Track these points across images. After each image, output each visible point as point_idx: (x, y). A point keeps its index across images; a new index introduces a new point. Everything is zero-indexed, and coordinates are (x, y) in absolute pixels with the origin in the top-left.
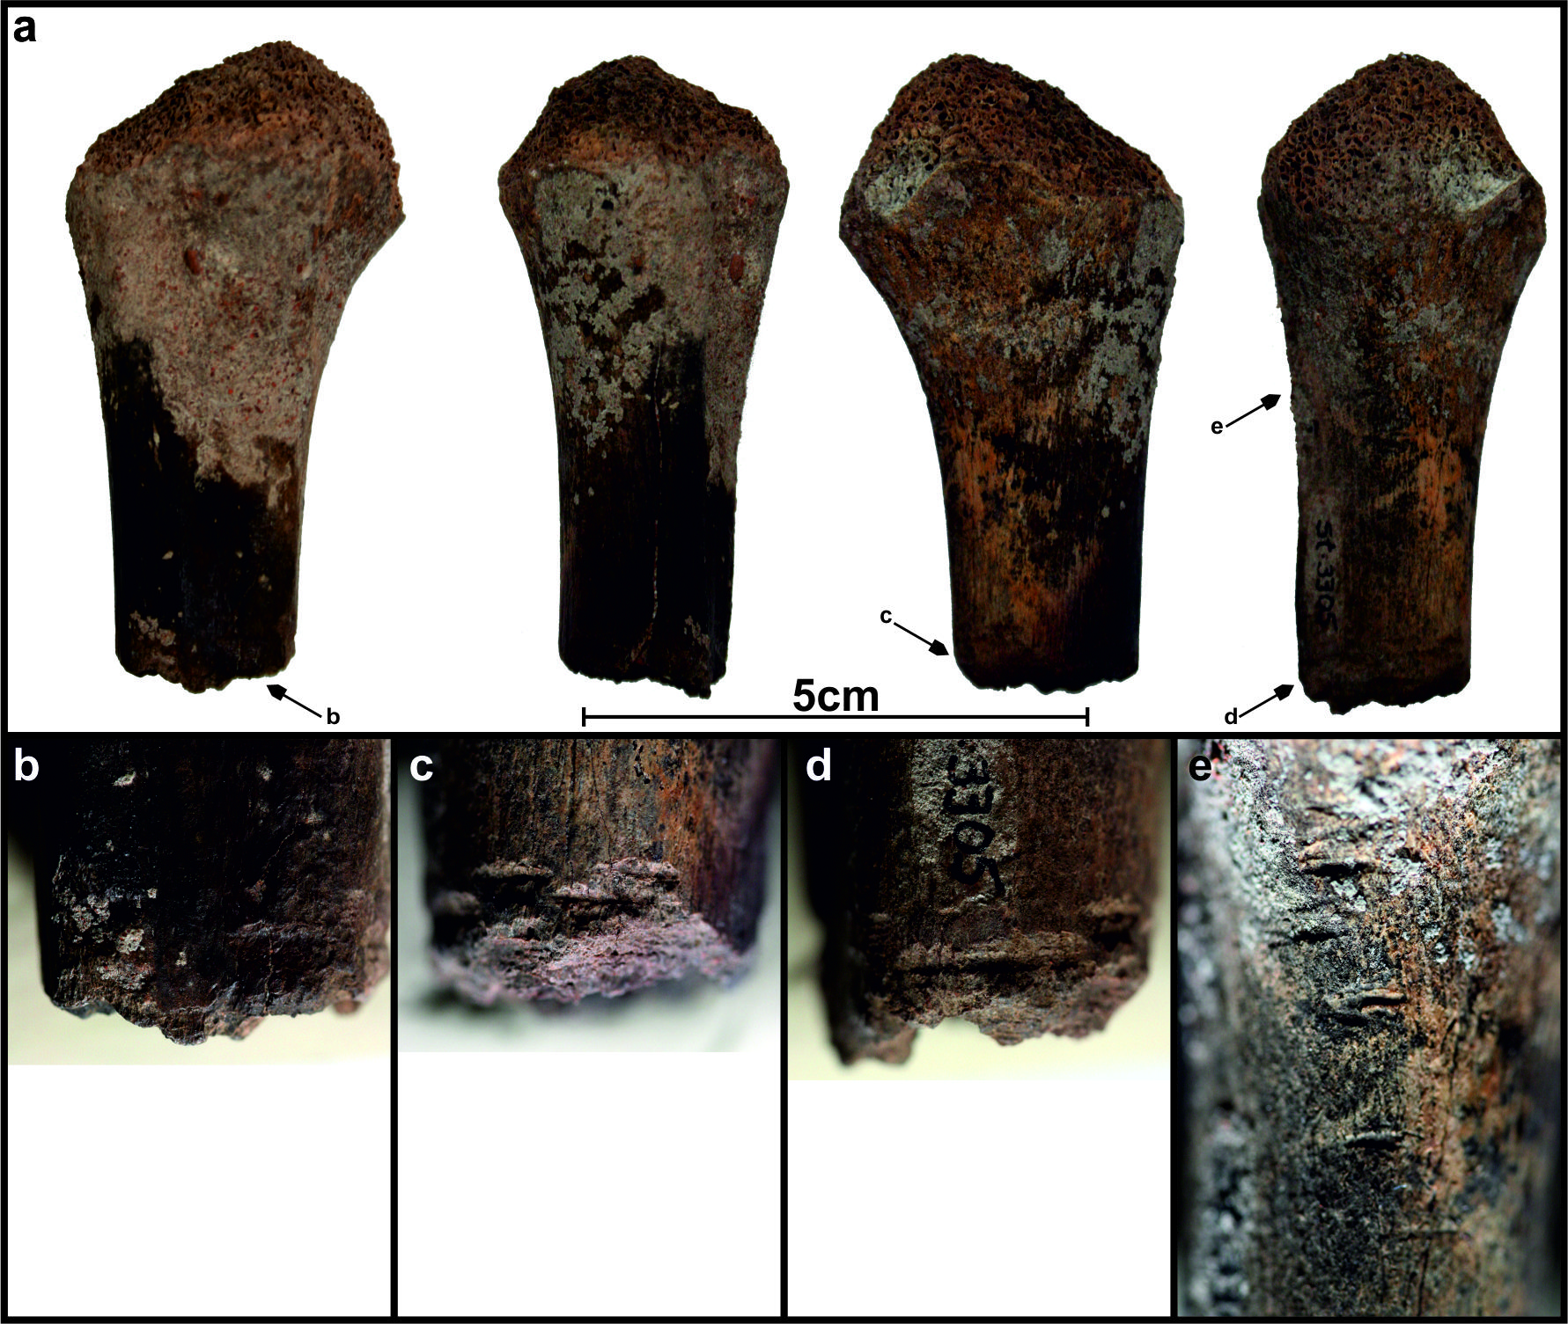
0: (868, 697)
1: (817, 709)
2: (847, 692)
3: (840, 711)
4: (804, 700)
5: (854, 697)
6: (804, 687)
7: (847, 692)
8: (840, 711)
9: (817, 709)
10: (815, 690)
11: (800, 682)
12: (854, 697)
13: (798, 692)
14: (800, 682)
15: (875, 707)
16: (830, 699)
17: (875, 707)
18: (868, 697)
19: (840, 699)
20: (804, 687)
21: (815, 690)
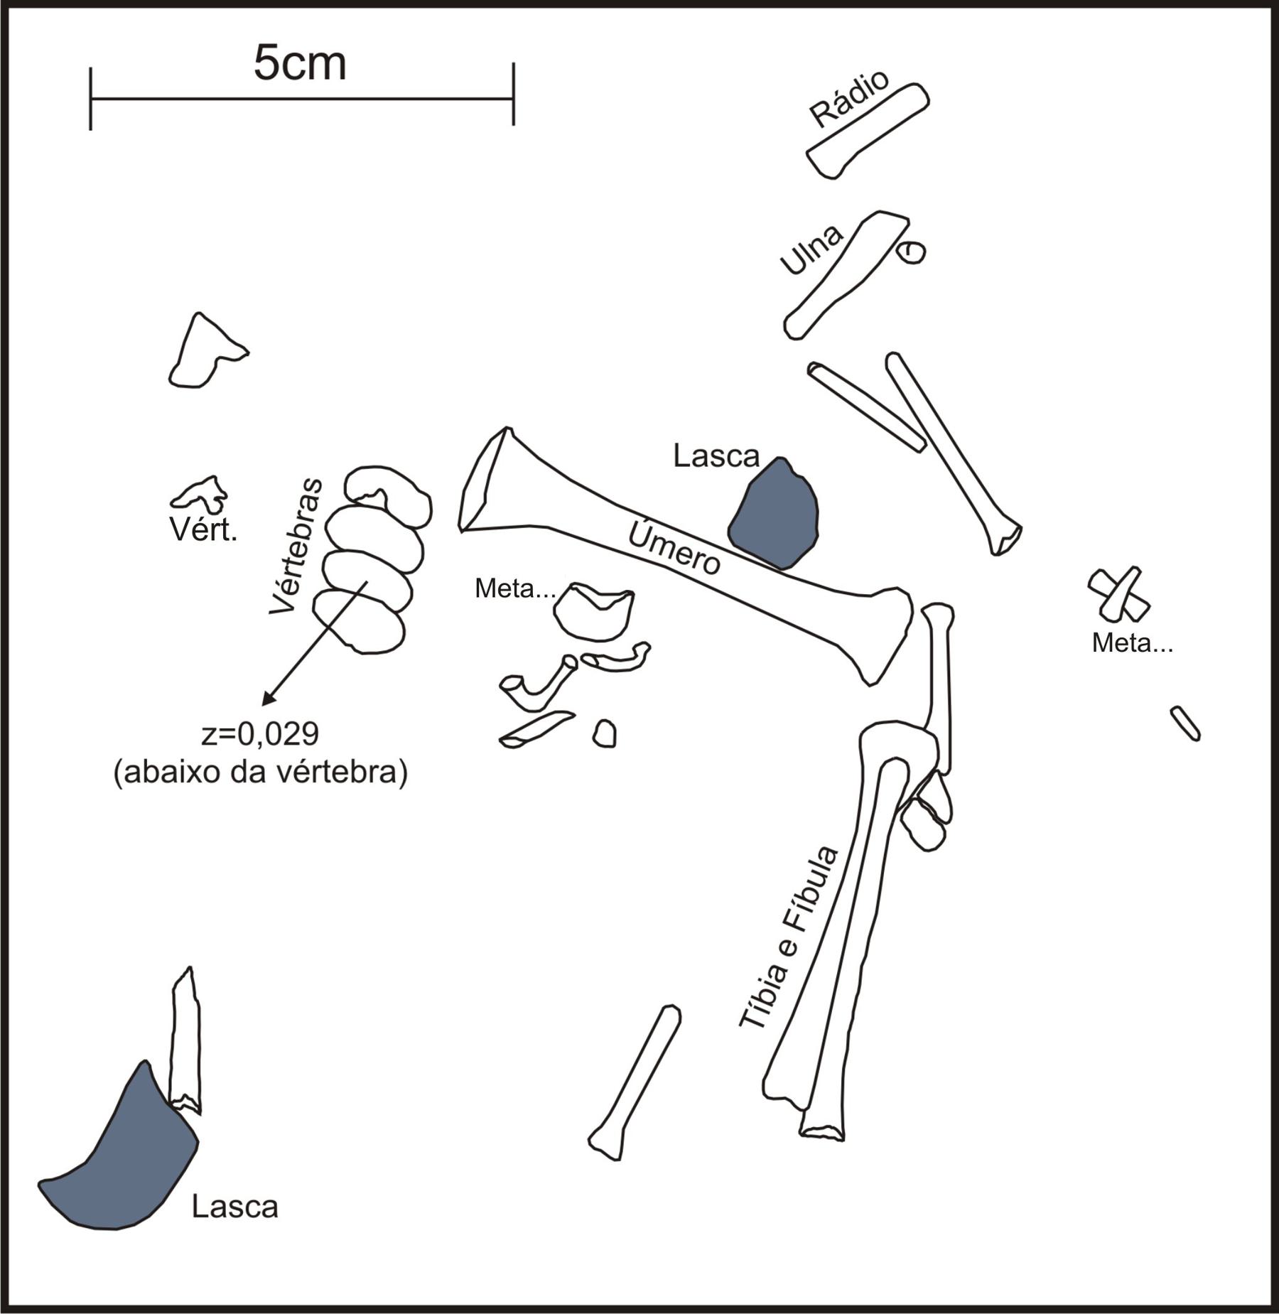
0: (335, 62)
2: (312, 58)
4: (267, 68)
5: (320, 62)
6: (266, 52)
7: (312, 58)
10: (280, 55)
11: (261, 47)
12: (320, 62)
13: (259, 59)
14: (261, 47)
16: (295, 66)
18: (335, 62)
19: (305, 65)
20: (266, 52)
21: (280, 55)
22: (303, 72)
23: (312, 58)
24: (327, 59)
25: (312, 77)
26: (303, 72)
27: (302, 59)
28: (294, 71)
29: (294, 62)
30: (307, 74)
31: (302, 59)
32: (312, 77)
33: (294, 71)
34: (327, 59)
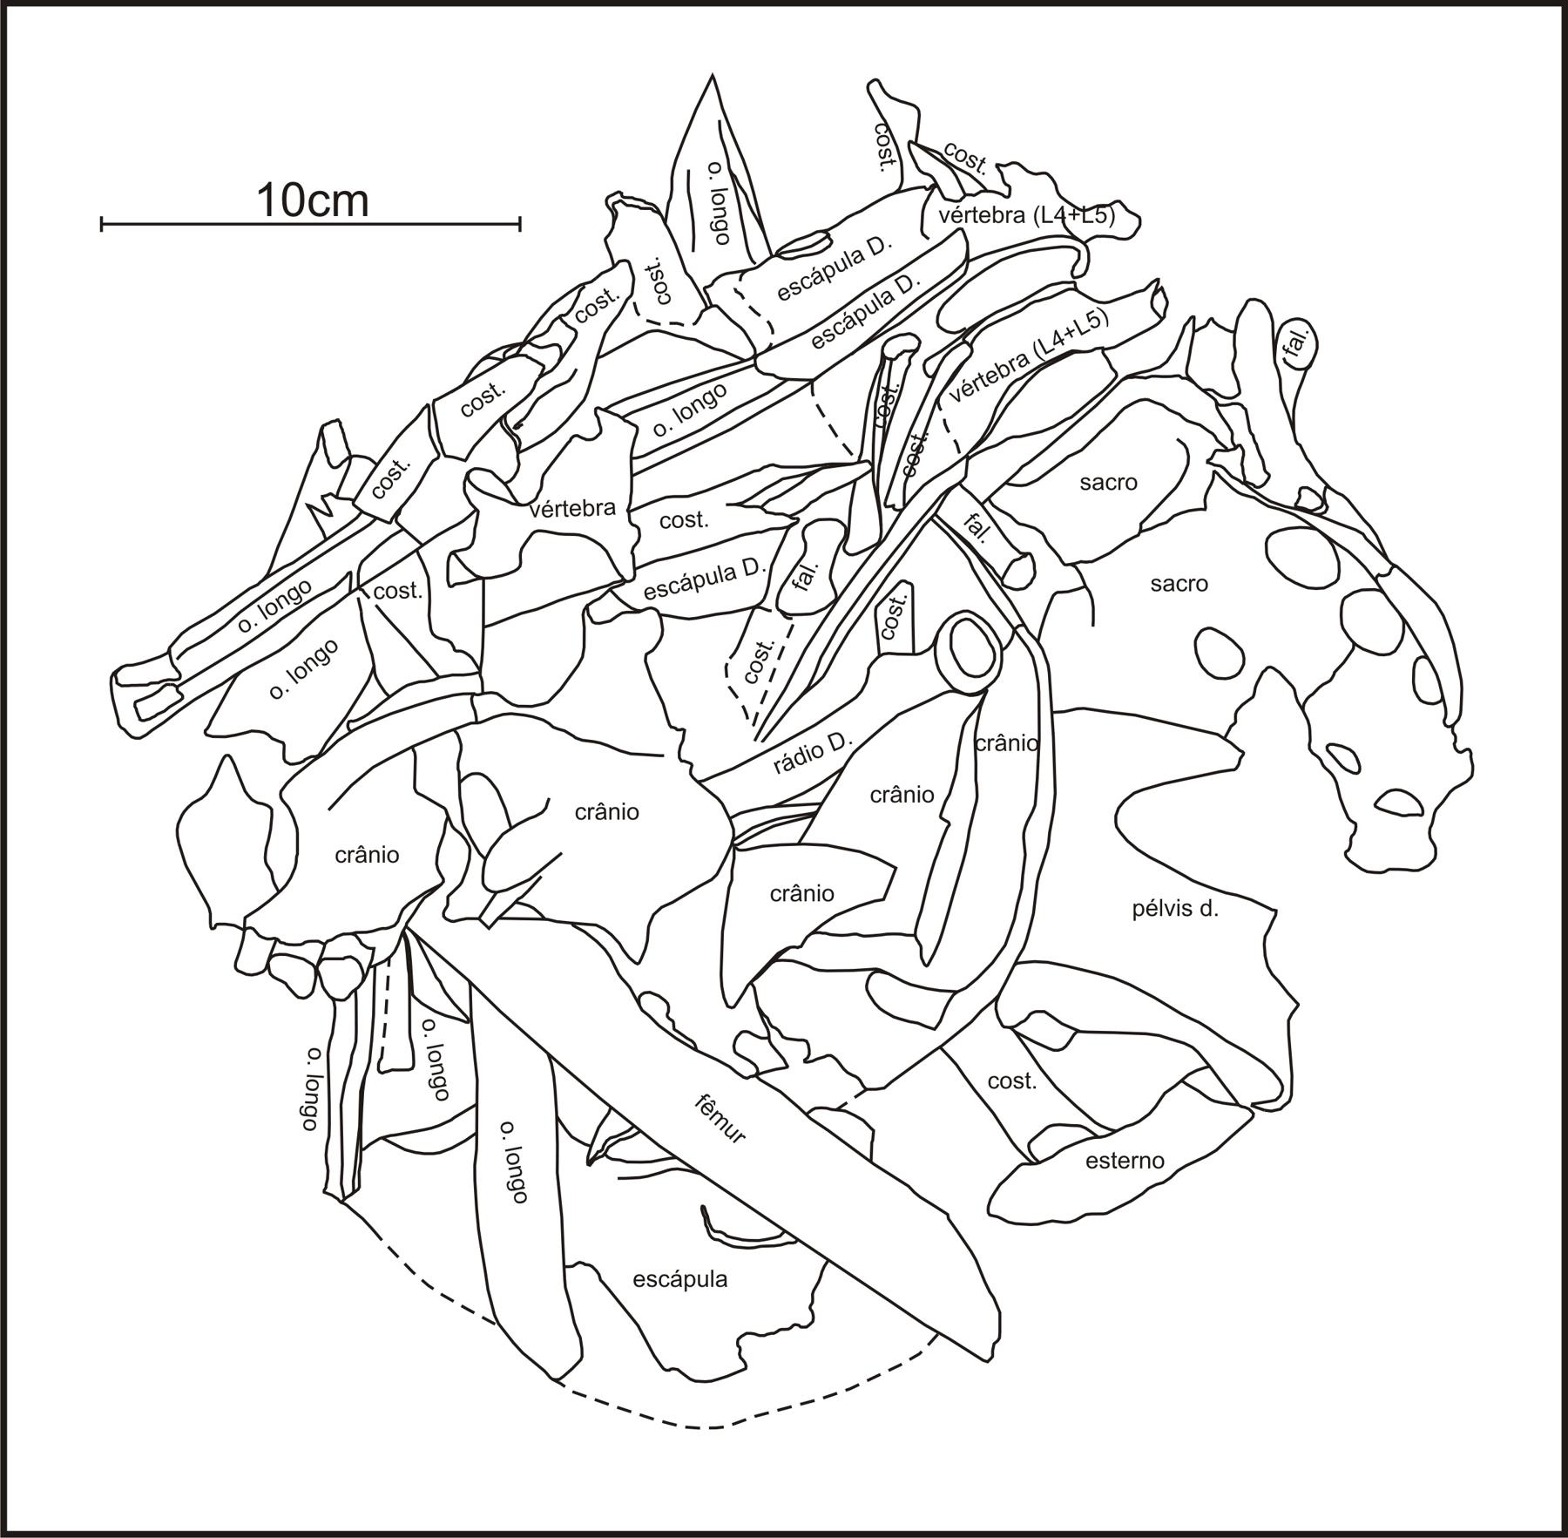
0: (358, 200)
1: (306, 216)
2: (337, 196)
3: (330, 218)
5: (343, 200)
8: (330, 218)
9: (306, 216)
12: (343, 200)
15: (365, 214)
16: (320, 204)
17: (365, 214)
18: (358, 200)
19: (330, 203)
22: (328, 210)
23: (337, 196)
24: (351, 197)
25: (336, 214)
26: (328, 210)
27: (327, 197)
28: (319, 208)
29: (319, 198)
30: (332, 211)
31: (327, 197)
32: (336, 214)
33: (319, 208)
34: (351, 197)
